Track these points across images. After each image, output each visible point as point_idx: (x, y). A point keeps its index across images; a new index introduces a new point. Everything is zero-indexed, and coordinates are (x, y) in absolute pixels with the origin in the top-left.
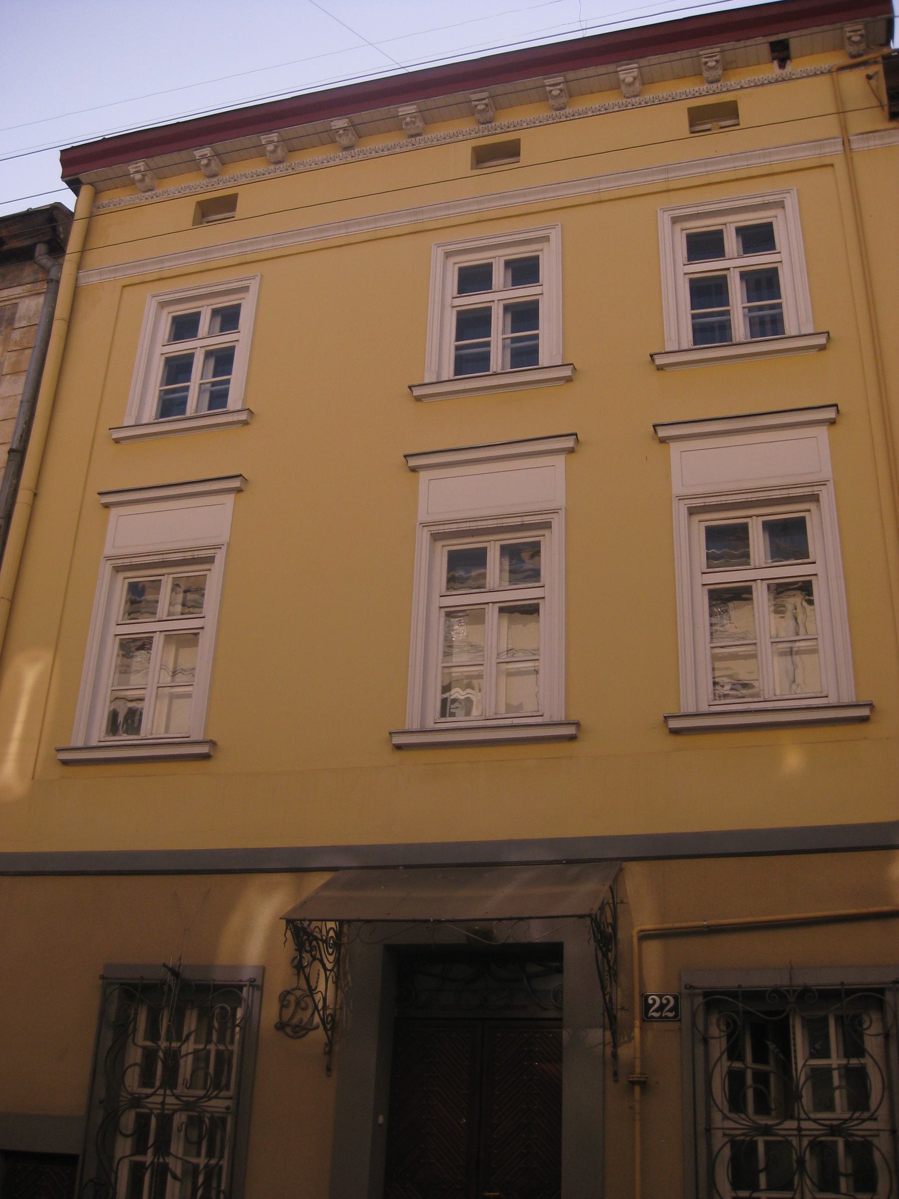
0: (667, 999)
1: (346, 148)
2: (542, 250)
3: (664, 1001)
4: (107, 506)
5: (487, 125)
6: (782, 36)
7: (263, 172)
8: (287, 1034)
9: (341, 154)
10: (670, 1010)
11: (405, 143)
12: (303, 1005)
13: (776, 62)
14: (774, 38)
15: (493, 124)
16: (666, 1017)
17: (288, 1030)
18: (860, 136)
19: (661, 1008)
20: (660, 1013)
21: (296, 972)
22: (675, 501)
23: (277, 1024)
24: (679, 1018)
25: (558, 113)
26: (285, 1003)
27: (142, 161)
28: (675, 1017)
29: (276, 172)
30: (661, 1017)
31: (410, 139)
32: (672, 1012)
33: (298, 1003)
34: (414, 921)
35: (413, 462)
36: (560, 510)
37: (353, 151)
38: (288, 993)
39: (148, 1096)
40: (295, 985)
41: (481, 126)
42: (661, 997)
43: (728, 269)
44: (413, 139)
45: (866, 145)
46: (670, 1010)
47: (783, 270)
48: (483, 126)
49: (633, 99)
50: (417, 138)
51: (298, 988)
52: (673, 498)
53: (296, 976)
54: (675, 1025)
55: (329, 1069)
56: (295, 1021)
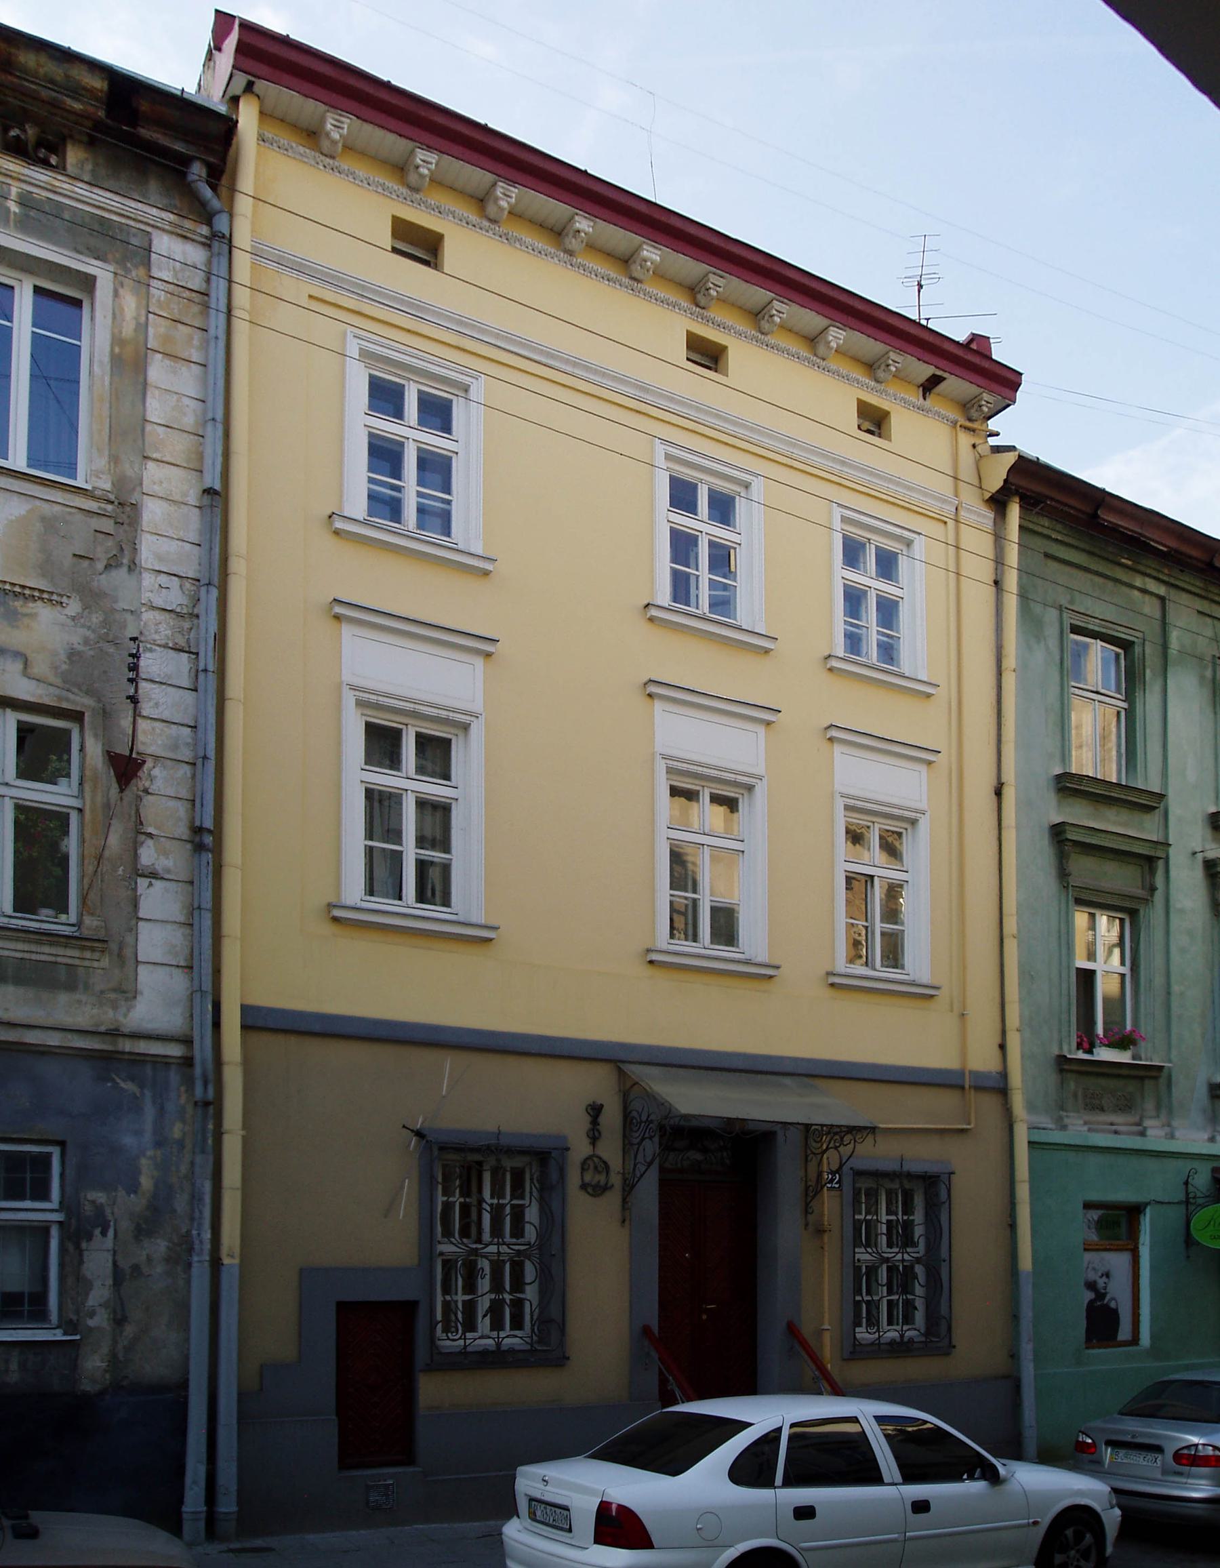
8: (588, 1193)
12: (600, 1169)
17: (590, 1190)
26: (586, 1167)
33: (596, 1168)
38: (587, 1159)
40: (591, 1153)
41: (698, 309)
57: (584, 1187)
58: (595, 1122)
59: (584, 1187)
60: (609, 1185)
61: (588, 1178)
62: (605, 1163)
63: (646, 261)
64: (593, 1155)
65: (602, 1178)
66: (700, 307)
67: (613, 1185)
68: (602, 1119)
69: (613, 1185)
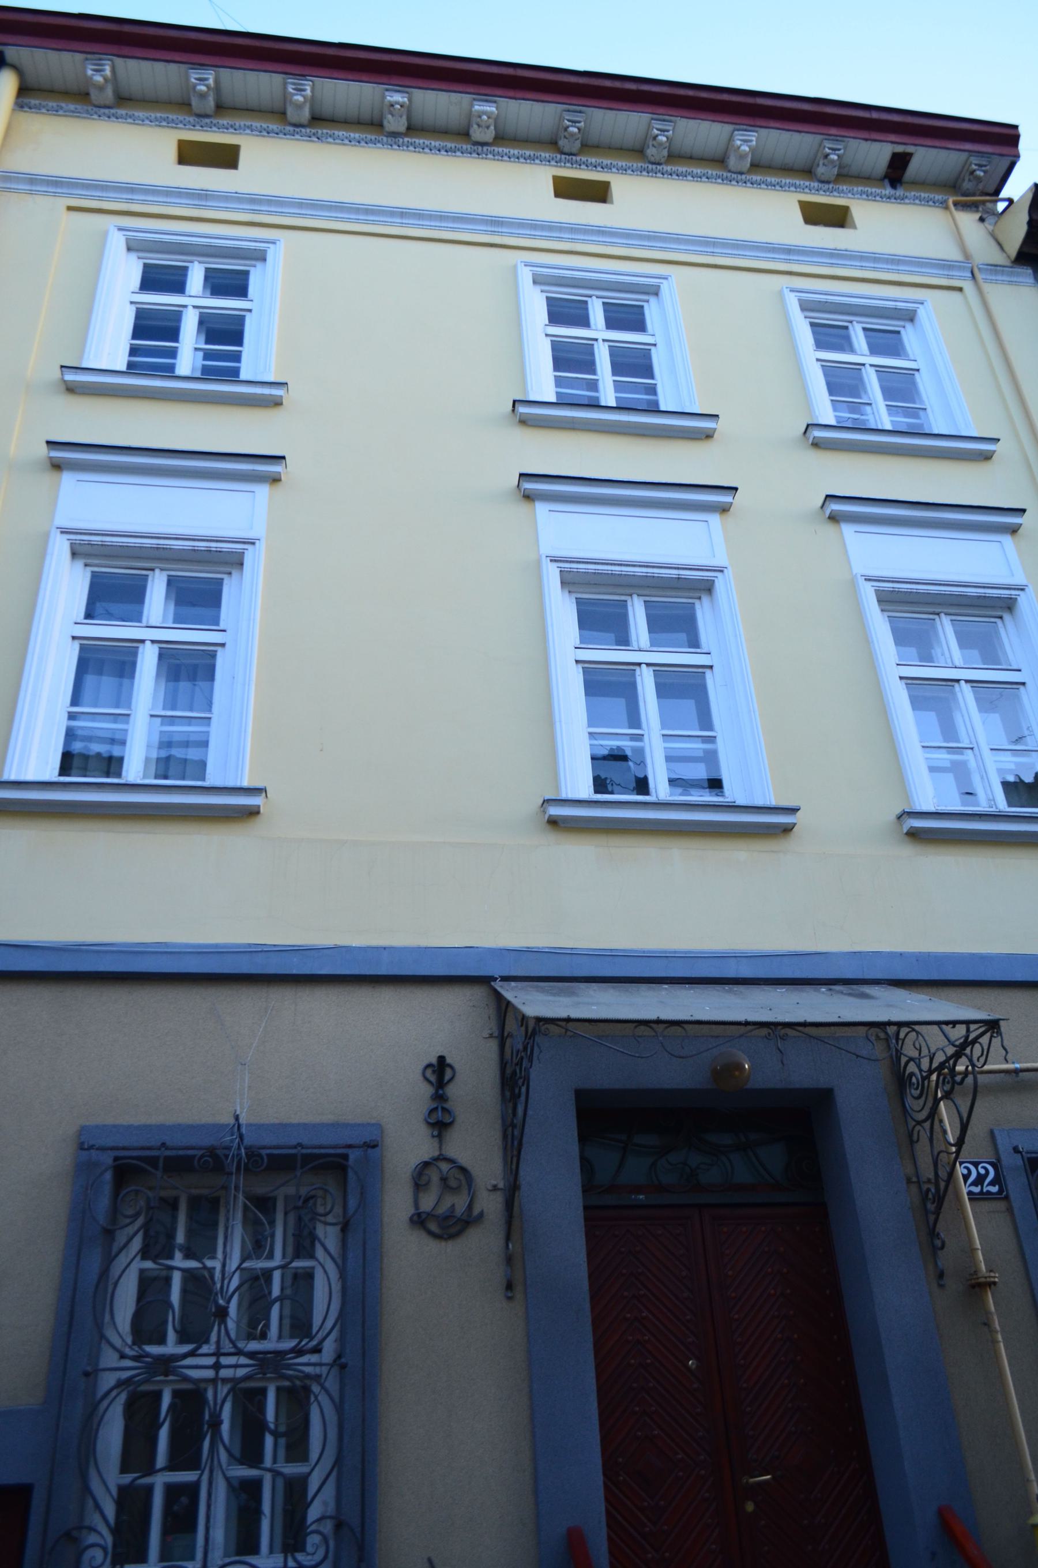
0: (984, 1168)
1: (394, 135)
2: (648, 301)
3: (982, 1171)
4: (57, 466)
5: (570, 157)
6: (910, 149)
7: (276, 130)
8: (430, 1233)
9: (385, 139)
10: (992, 1183)
11: (469, 149)
12: (453, 1183)
13: (887, 181)
14: (900, 149)
15: (578, 158)
16: (989, 1193)
17: (433, 1227)
18: (989, 267)
19: (980, 1180)
20: (980, 1187)
21: (436, 1133)
22: (861, 581)
23: (413, 1216)
24: (1005, 1193)
25: (654, 167)
27: (109, 60)
28: (1000, 1191)
29: (294, 135)
30: (981, 1193)
31: (476, 148)
32: (994, 1186)
33: (444, 1180)
34: (747, 1023)
35: (529, 486)
36: (725, 569)
37: (401, 140)
38: (426, 1164)
39: (185, 1356)
40: (436, 1153)
41: (563, 156)
42: (976, 1165)
43: (864, 365)
44: (480, 148)
45: (994, 278)
46: (992, 1183)
47: (922, 380)
48: (567, 157)
49: (739, 176)
50: (485, 148)
51: (441, 1157)
52: (859, 576)
53: (436, 1140)
54: (1001, 1205)
55: (509, 1286)
56: (441, 1210)
57: (419, 1220)
58: (439, 1097)
59: (419, 1220)
60: (476, 1212)
61: (427, 1203)
62: (463, 1170)
63: (480, 117)
64: (442, 1158)
65: (459, 1203)
66: (565, 154)
67: (481, 1215)
68: (452, 1091)
69: (481, 1215)
